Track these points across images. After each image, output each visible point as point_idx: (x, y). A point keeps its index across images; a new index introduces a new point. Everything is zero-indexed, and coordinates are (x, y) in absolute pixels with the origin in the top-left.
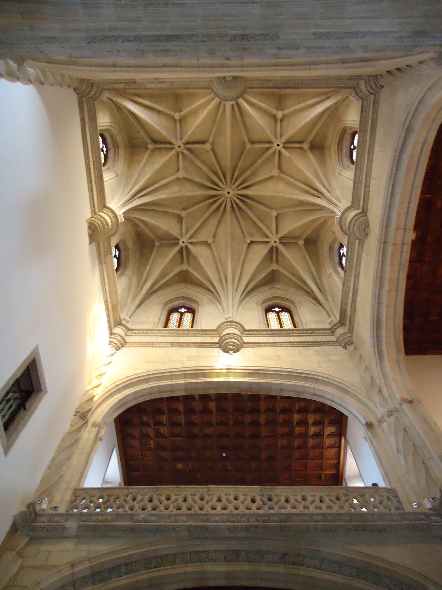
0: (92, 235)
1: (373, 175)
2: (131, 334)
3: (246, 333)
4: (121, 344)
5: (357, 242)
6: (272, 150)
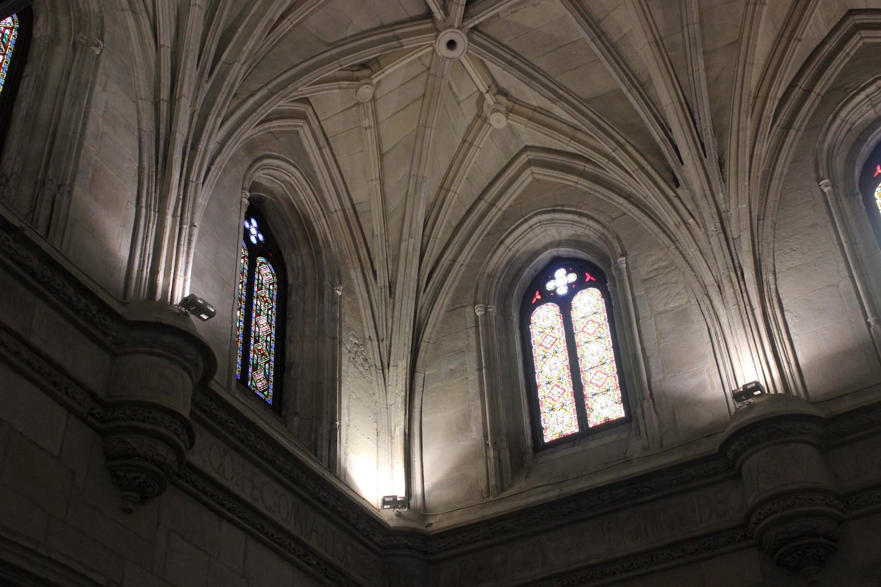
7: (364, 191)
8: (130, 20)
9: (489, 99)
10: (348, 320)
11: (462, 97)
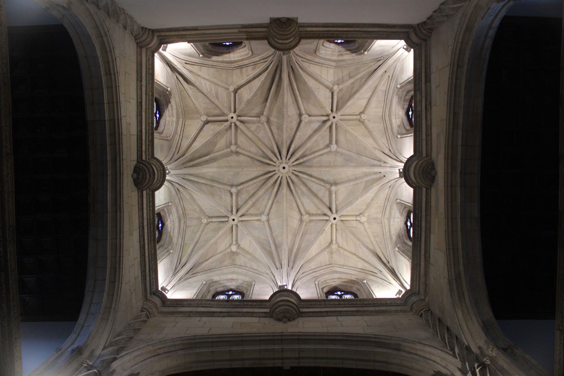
0: (280, 21)
1: (340, 318)
2: (148, 54)
3: (151, 193)
4: (140, 42)
5: (267, 310)
6: (329, 213)
7: (360, 264)
8: (261, 276)
9: (358, 218)
10: (369, 283)
11: (355, 226)
